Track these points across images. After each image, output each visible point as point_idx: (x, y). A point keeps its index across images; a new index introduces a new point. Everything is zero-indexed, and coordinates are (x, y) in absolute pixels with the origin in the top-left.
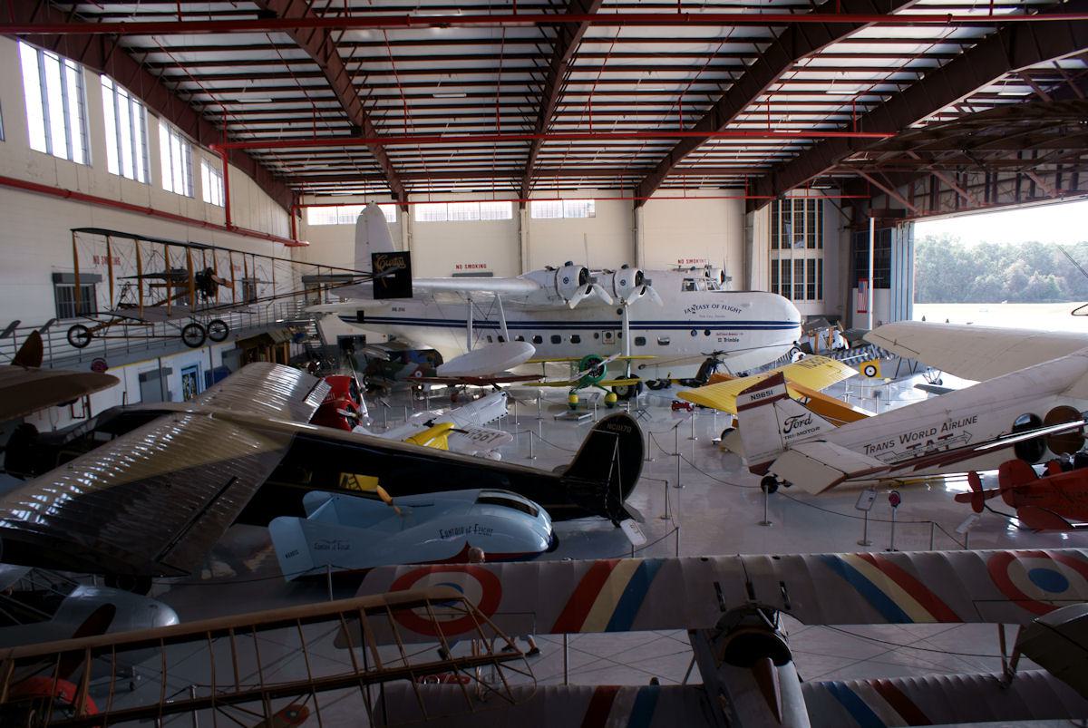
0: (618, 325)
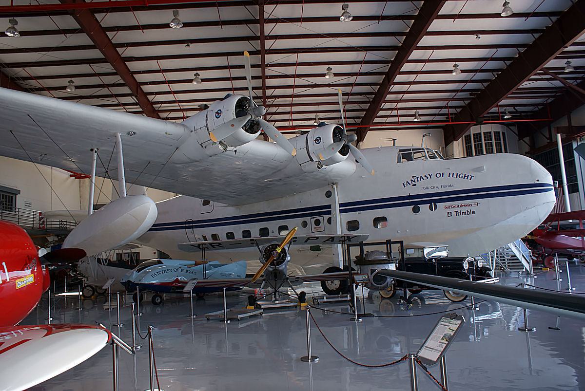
0: (325, 210)
